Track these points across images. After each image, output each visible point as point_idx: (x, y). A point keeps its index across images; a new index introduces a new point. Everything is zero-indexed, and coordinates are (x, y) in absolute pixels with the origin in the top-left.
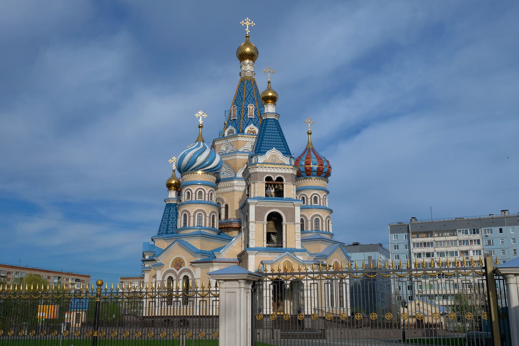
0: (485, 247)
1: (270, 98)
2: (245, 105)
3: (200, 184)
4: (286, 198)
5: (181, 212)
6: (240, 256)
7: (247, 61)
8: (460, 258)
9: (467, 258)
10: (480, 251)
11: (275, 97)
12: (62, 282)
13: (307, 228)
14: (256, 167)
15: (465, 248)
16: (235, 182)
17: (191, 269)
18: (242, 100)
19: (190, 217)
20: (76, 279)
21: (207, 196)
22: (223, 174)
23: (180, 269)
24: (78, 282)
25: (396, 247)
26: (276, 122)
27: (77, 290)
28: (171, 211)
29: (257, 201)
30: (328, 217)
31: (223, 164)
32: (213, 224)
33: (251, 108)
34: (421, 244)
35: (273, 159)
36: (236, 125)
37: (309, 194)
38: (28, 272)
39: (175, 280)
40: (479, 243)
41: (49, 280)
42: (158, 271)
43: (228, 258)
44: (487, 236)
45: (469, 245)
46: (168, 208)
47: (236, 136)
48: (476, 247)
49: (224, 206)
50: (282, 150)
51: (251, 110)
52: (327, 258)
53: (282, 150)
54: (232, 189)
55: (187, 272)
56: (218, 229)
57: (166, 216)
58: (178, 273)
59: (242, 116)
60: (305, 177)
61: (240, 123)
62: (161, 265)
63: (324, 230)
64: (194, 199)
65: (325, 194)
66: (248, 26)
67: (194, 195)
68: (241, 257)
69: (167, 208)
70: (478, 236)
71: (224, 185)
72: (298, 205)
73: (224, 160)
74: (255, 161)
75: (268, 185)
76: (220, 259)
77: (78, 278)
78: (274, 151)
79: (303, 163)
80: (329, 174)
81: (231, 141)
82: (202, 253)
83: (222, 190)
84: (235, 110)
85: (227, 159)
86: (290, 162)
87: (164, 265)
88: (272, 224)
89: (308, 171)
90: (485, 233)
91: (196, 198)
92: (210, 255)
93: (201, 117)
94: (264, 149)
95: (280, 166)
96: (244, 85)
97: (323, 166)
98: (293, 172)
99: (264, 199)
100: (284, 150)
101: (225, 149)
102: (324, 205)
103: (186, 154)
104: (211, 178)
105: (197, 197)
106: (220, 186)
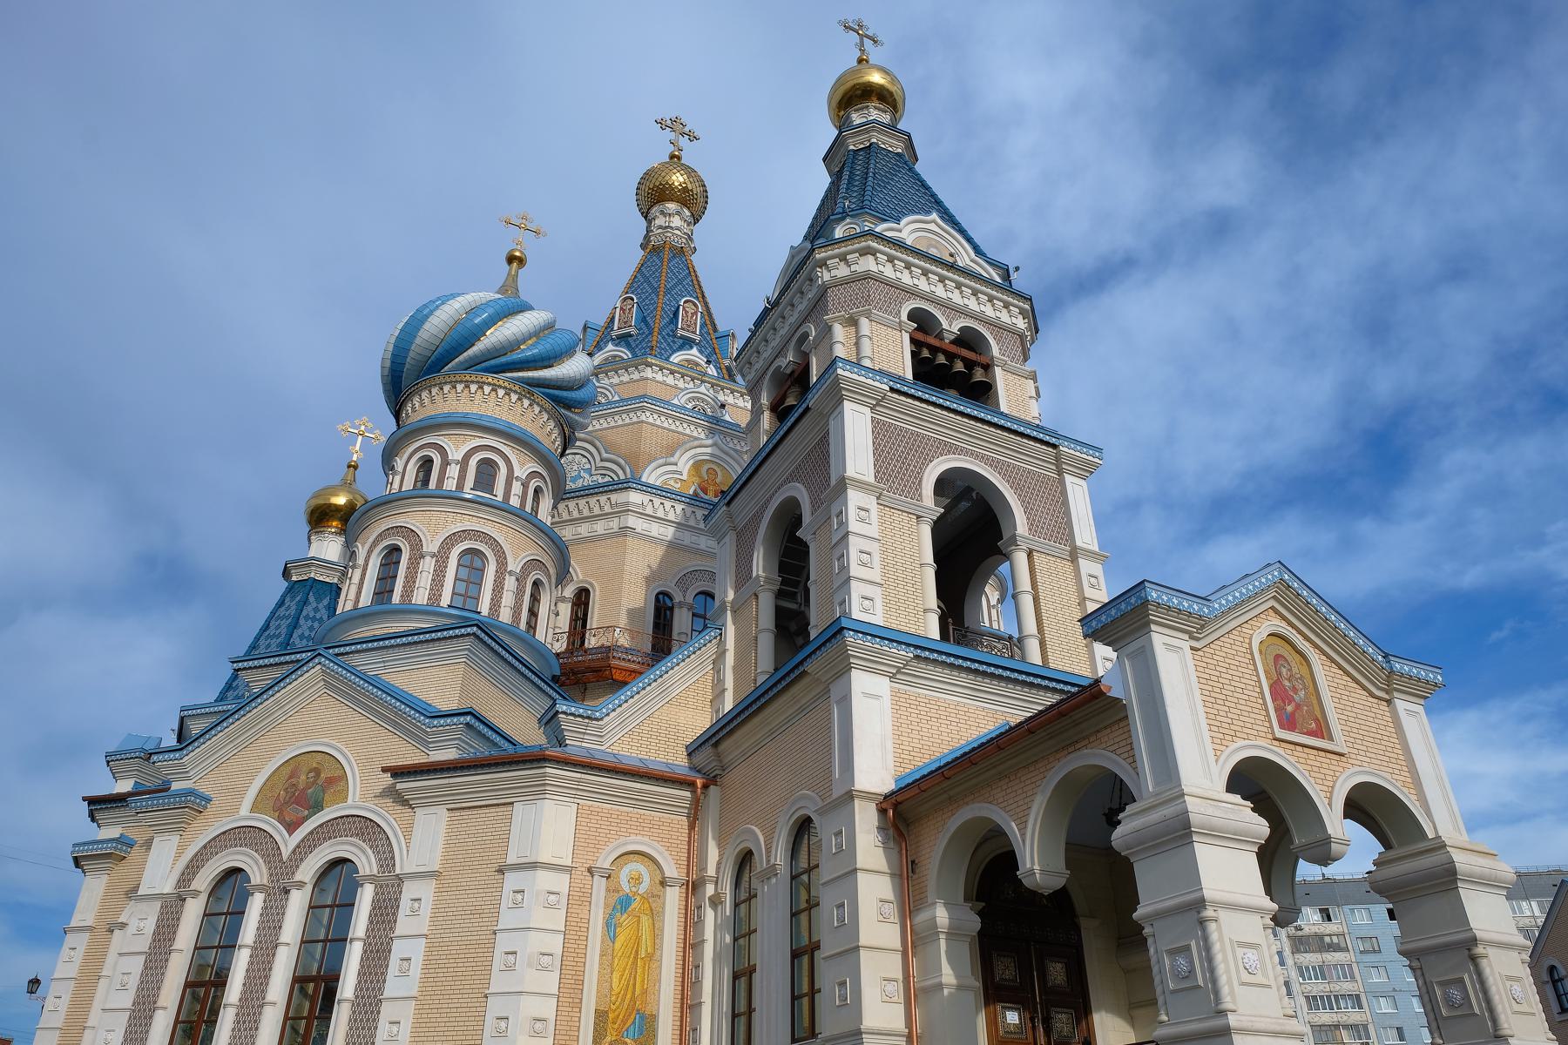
6: (716, 745)
7: (672, 206)
16: (635, 497)
17: (387, 817)
23: (306, 819)
28: (308, 610)
31: (599, 390)
42: (166, 837)
43: (634, 753)
46: (293, 598)
49: (569, 592)
54: (614, 524)
57: (278, 627)
58: (288, 843)
68: (722, 747)
69: (288, 599)
71: (580, 511)
78: (932, 227)
87: (208, 800)
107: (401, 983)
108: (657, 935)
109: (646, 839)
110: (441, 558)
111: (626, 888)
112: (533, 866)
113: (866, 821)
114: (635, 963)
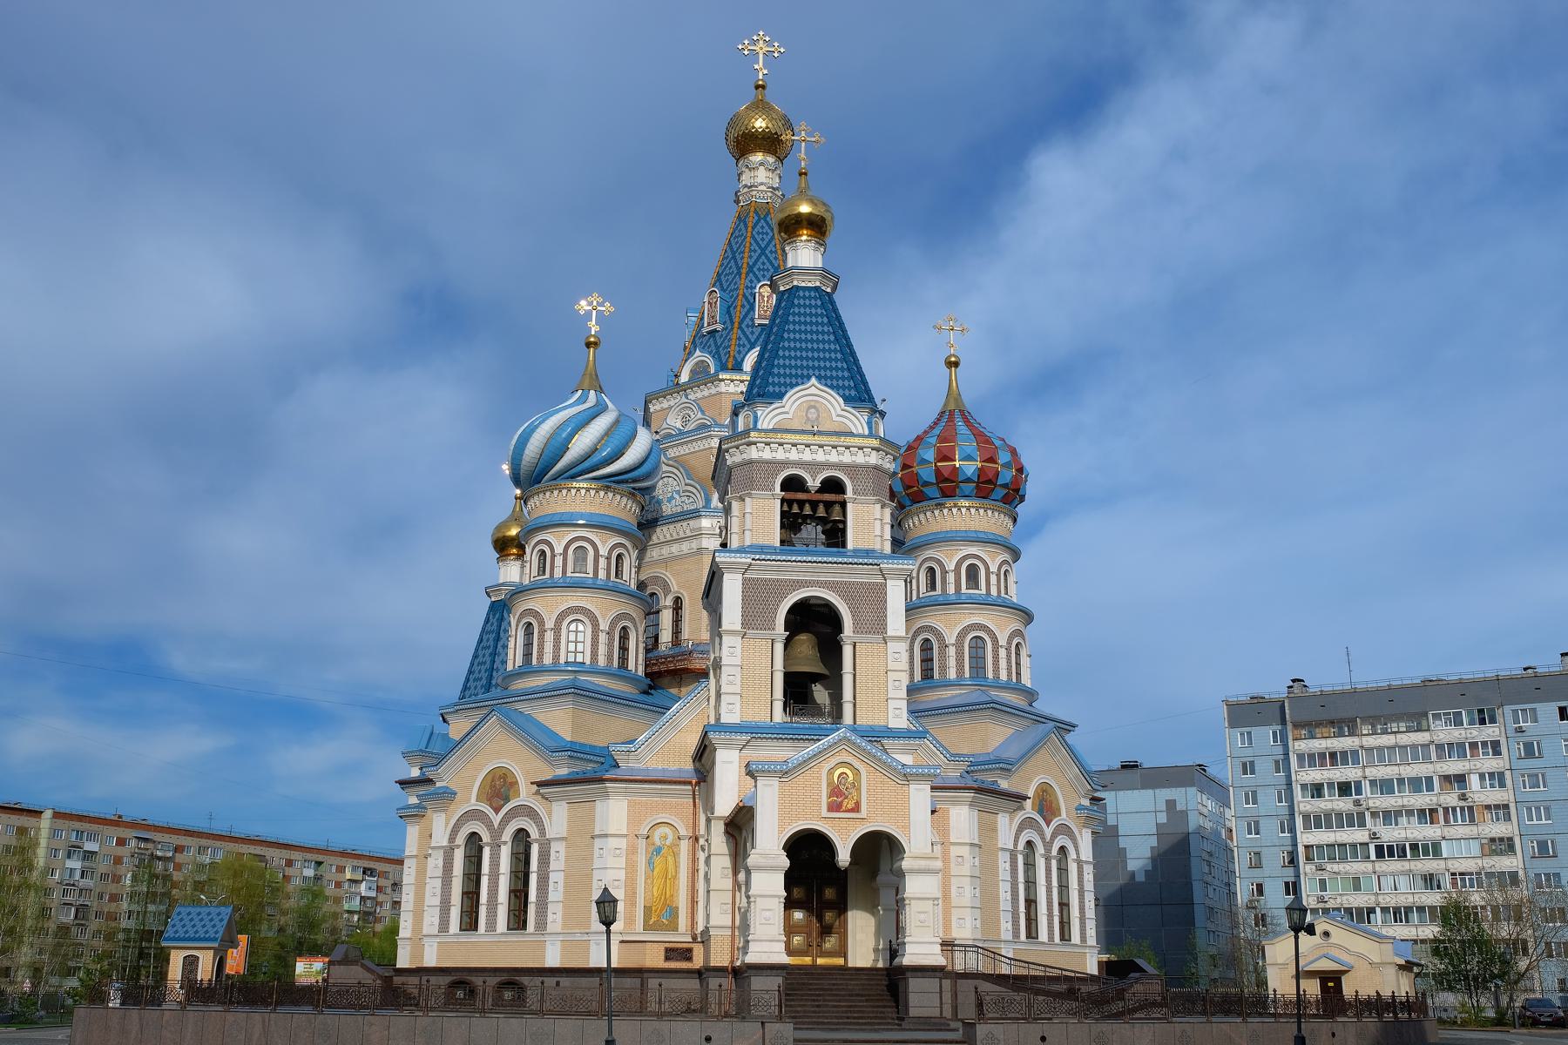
0: (1517, 764)
1: (805, 223)
2: (747, 287)
3: (581, 522)
4: (855, 551)
5: (517, 617)
7: (758, 157)
8: (1442, 798)
9: (1463, 797)
10: (1501, 775)
11: (823, 220)
12: (327, 876)
13: (943, 668)
14: (749, 444)
15: (1454, 766)
18: (739, 274)
19: (542, 632)
20: (364, 868)
21: (602, 563)
22: (670, 499)
24: (371, 875)
25: (1248, 768)
26: (826, 301)
27: (369, 898)
29: (749, 560)
30: (1018, 633)
32: (623, 659)
33: (766, 294)
34: (1322, 755)
35: (810, 416)
36: (718, 347)
37: (950, 558)
38: (231, 846)
39: (488, 844)
40: (1497, 752)
41: (289, 871)
44: (1520, 730)
45: (1469, 758)
46: (494, 615)
47: (715, 379)
48: (1490, 764)
49: (669, 602)
51: (766, 299)
52: (1009, 770)
53: (844, 388)
54: (694, 545)
55: (526, 818)
56: (641, 672)
57: (488, 640)
58: (496, 819)
59: (737, 320)
60: (937, 501)
61: (730, 340)
62: (448, 796)
63: (1003, 676)
64: (558, 573)
65: (1006, 556)
66: (761, 56)
67: (559, 561)
68: (703, 761)
69: (491, 617)
70: (1493, 732)
72: (897, 574)
73: (673, 455)
74: (746, 424)
75: (790, 507)
76: (632, 769)
77: (367, 866)
78: (813, 390)
79: (930, 455)
80: (1017, 491)
81: (699, 395)
82: (575, 751)
83: (665, 551)
84: (716, 303)
85: (682, 452)
86: (870, 428)
88: (805, 642)
89: (946, 480)
90: (1516, 721)
91: (564, 572)
92: (602, 760)
93: (594, 312)
94: (780, 385)
95: (834, 440)
96: (746, 227)
97: (996, 463)
98: (880, 462)
99: (776, 554)
100: (849, 388)
101: (678, 425)
102: (1003, 595)
103: (537, 427)
104: (620, 507)
105: (570, 568)
106: (658, 539)
107: (555, 894)
108: (677, 867)
109: (667, 815)
110: (557, 630)
111: (658, 843)
112: (606, 836)
113: (718, 829)
114: (666, 881)
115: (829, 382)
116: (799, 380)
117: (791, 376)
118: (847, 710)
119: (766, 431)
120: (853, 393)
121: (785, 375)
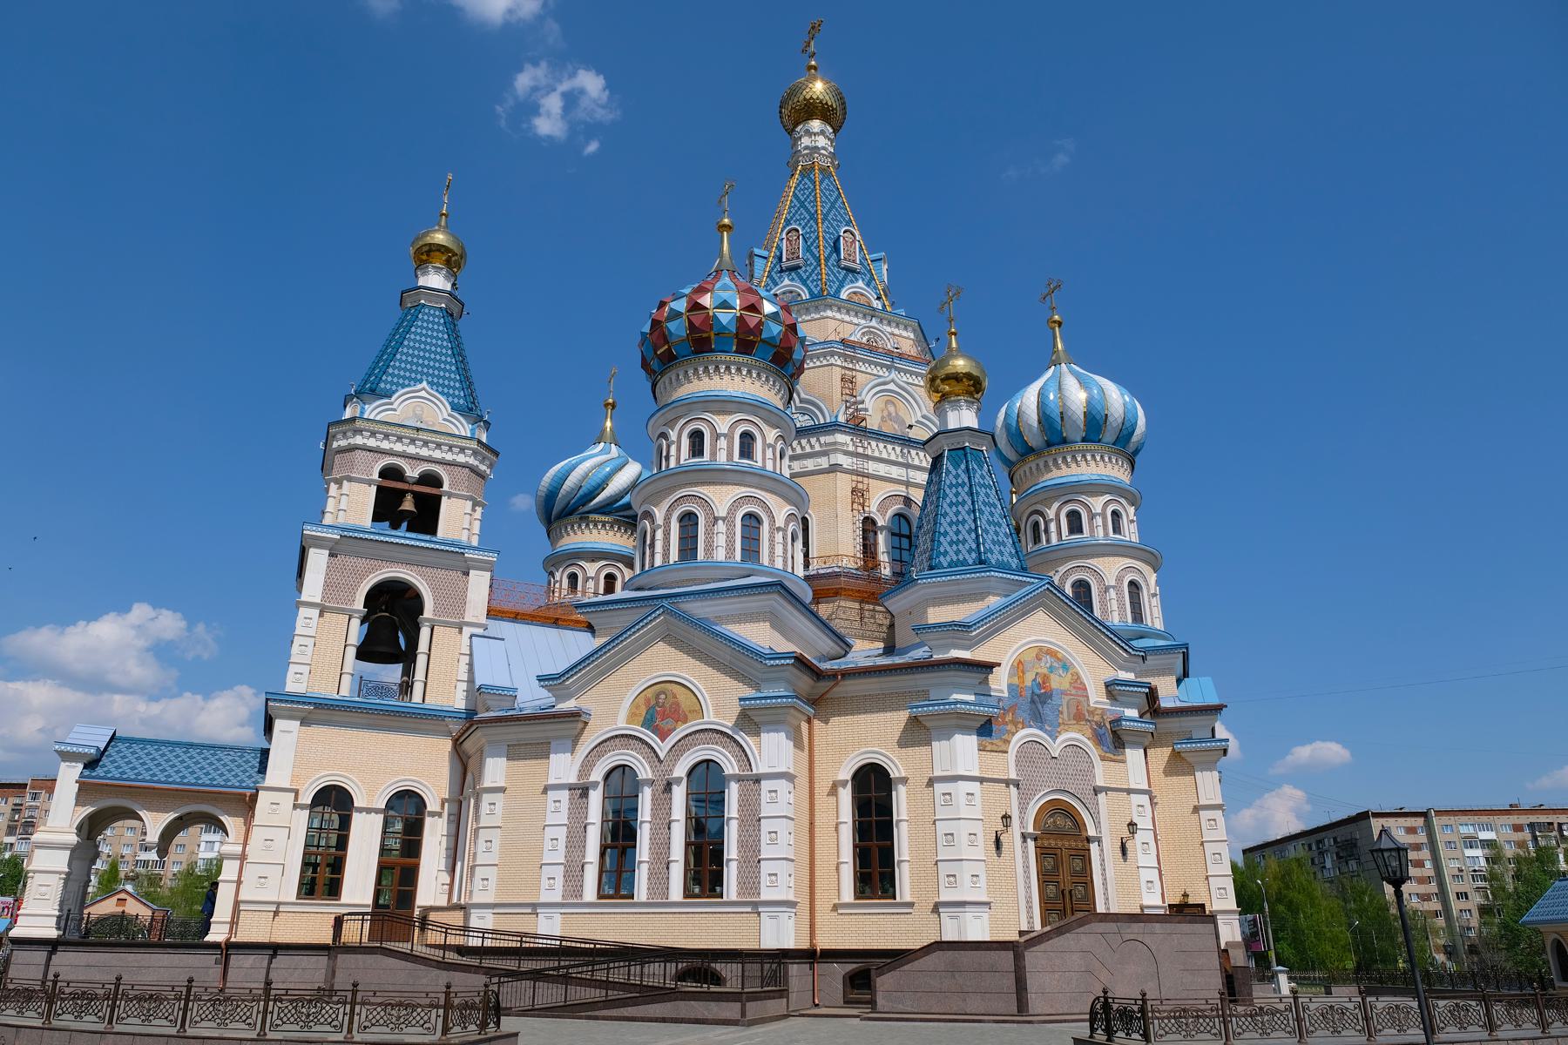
50: (454, 396)
53: (454, 396)
78: (423, 394)
94: (392, 383)
100: (459, 397)
115: (440, 389)
116: (412, 383)
117: (404, 378)
118: (418, 688)
119: (368, 420)
120: (462, 401)
121: (399, 376)
